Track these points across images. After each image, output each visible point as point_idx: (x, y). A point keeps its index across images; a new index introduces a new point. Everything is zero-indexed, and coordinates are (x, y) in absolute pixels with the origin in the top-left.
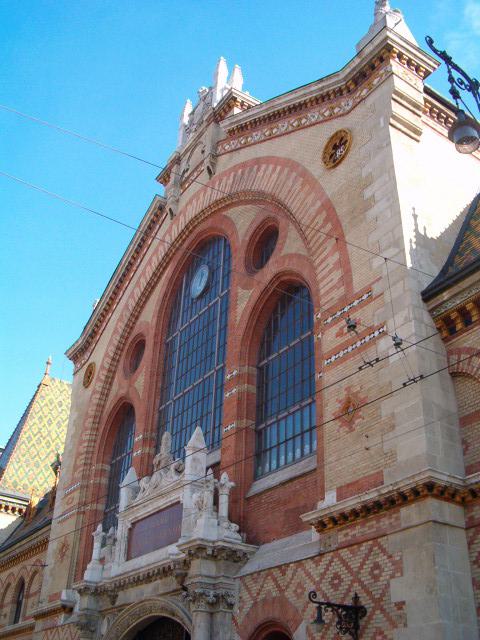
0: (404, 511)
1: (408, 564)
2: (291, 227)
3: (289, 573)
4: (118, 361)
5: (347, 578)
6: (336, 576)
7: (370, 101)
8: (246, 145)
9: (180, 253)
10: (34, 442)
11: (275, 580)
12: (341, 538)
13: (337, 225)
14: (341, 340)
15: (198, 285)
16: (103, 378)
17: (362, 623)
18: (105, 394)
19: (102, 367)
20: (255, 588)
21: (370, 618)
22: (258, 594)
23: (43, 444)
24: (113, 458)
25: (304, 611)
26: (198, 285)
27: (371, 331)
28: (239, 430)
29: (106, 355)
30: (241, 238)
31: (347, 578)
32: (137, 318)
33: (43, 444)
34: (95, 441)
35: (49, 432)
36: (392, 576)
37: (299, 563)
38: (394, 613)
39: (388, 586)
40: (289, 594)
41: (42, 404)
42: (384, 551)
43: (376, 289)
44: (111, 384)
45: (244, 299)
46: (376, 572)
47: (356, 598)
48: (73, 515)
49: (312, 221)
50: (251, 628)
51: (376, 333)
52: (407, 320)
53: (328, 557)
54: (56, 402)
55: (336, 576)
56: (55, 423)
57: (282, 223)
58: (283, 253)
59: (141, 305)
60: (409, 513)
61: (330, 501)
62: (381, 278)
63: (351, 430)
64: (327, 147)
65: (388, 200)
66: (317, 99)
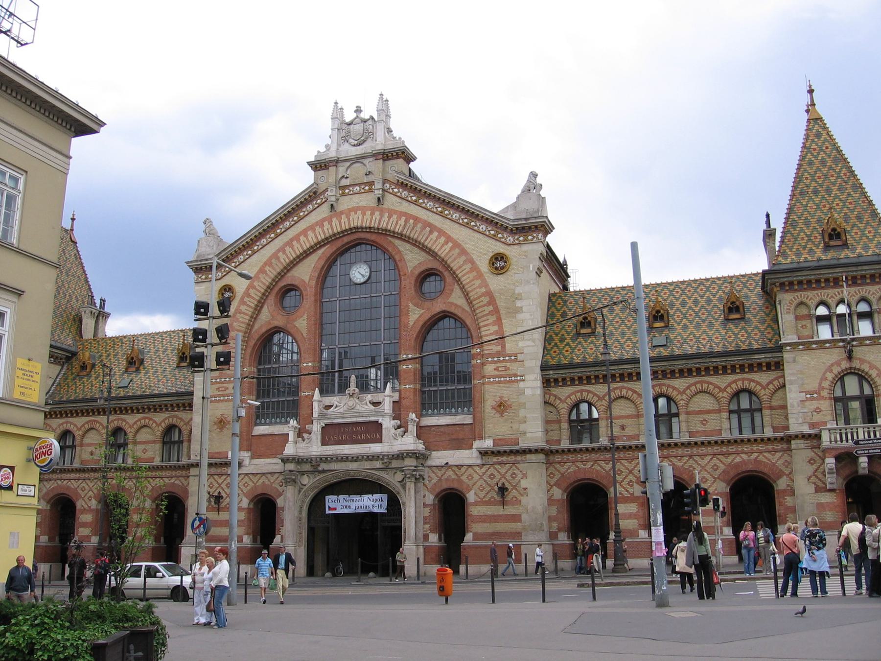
0: (528, 456)
1: (530, 474)
2: (456, 286)
3: (463, 469)
4: (267, 297)
6: (492, 474)
7: (525, 248)
8: (415, 203)
9: (339, 243)
11: (454, 471)
12: (495, 459)
13: (496, 311)
14: (497, 373)
15: (359, 273)
16: (253, 305)
17: (506, 493)
18: (255, 317)
19: (247, 294)
20: (440, 474)
21: (510, 492)
22: (442, 476)
23: (61, 294)
24: (260, 364)
25: (473, 486)
26: (359, 273)
27: (516, 375)
28: (415, 389)
32: (288, 271)
33: (61, 294)
34: (245, 350)
36: (522, 478)
37: (470, 466)
38: (522, 492)
39: (520, 481)
40: (464, 478)
42: (518, 469)
43: (520, 357)
44: (259, 311)
45: (415, 315)
46: (514, 476)
47: (503, 484)
48: (228, 400)
49: (480, 297)
50: (438, 490)
51: (519, 378)
52: (536, 379)
53: (488, 466)
57: (449, 279)
58: (451, 300)
60: (529, 457)
61: (488, 444)
62: (523, 353)
64: (492, 258)
65: (531, 315)
66: (487, 219)
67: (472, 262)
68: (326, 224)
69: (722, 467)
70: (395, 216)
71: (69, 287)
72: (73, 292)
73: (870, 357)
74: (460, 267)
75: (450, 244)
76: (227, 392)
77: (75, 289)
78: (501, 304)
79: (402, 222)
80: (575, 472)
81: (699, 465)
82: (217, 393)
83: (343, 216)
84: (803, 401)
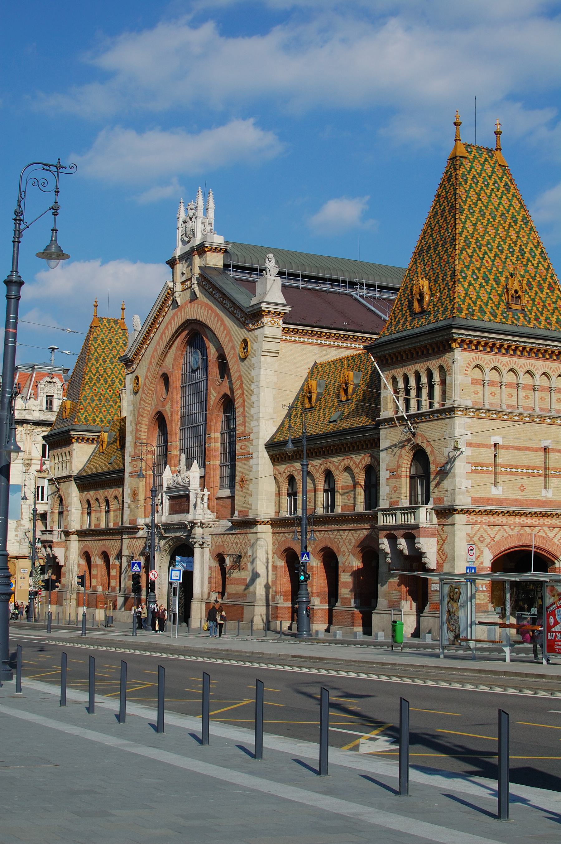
5: (239, 544)
6: (237, 543)
7: (257, 332)
10: (94, 381)
13: (243, 394)
19: (145, 384)
23: (102, 381)
29: (147, 377)
30: (212, 355)
31: (239, 544)
33: (102, 381)
35: (105, 369)
41: (96, 346)
54: (106, 340)
55: (237, 543)
56: (108, 360)
59: (165, 354)
63: (242, 491)
67: (233, 347)
68: (176, 317)
69: (353, 541)
70: (203, 307)
71: (112, 372)
72: (117, 377)
73: (427, 435)
74: (229, 353)
75: (225, 332)
76: (137, 469)
77: (119, 373)
78: (245, 387)
79: (206, 313)
80: (284, 541)
81: (342, 538)
82: (134, 469)
83: (183, 310)
84: (387, 479)
